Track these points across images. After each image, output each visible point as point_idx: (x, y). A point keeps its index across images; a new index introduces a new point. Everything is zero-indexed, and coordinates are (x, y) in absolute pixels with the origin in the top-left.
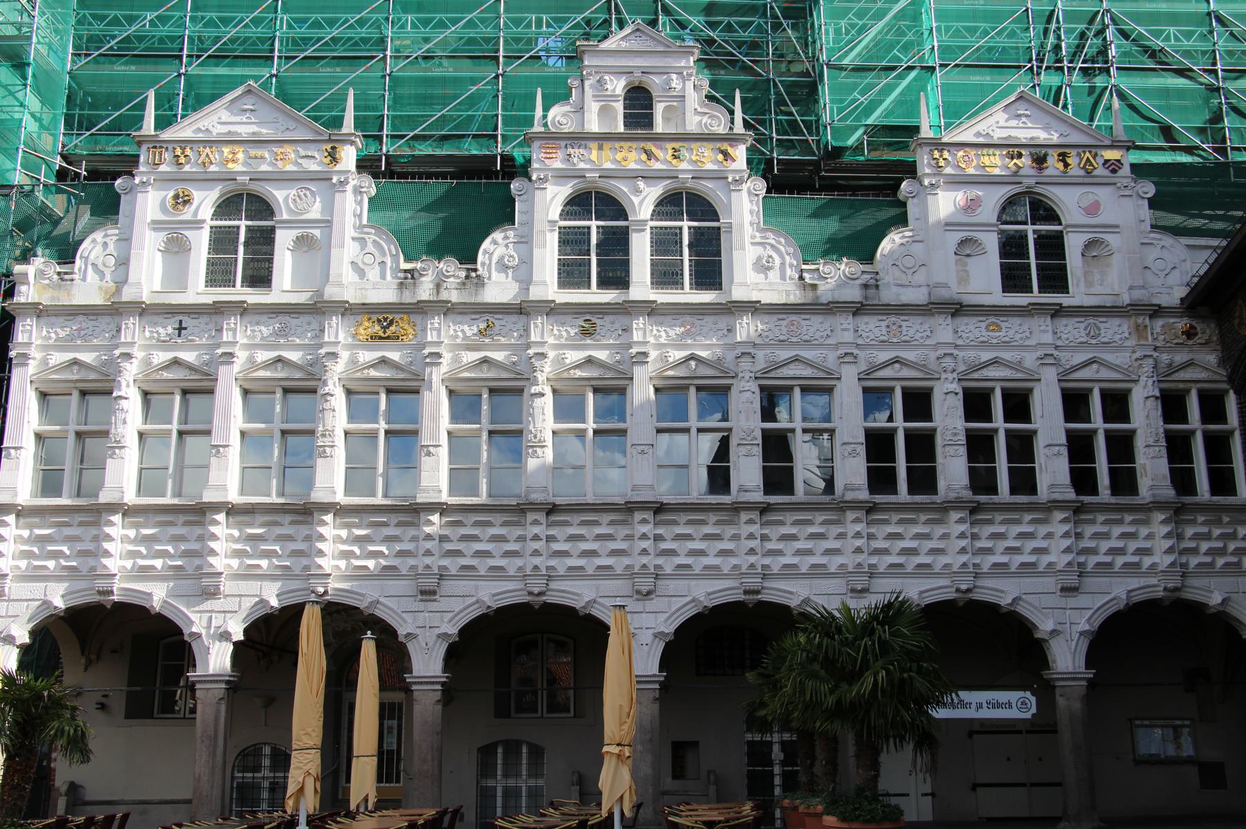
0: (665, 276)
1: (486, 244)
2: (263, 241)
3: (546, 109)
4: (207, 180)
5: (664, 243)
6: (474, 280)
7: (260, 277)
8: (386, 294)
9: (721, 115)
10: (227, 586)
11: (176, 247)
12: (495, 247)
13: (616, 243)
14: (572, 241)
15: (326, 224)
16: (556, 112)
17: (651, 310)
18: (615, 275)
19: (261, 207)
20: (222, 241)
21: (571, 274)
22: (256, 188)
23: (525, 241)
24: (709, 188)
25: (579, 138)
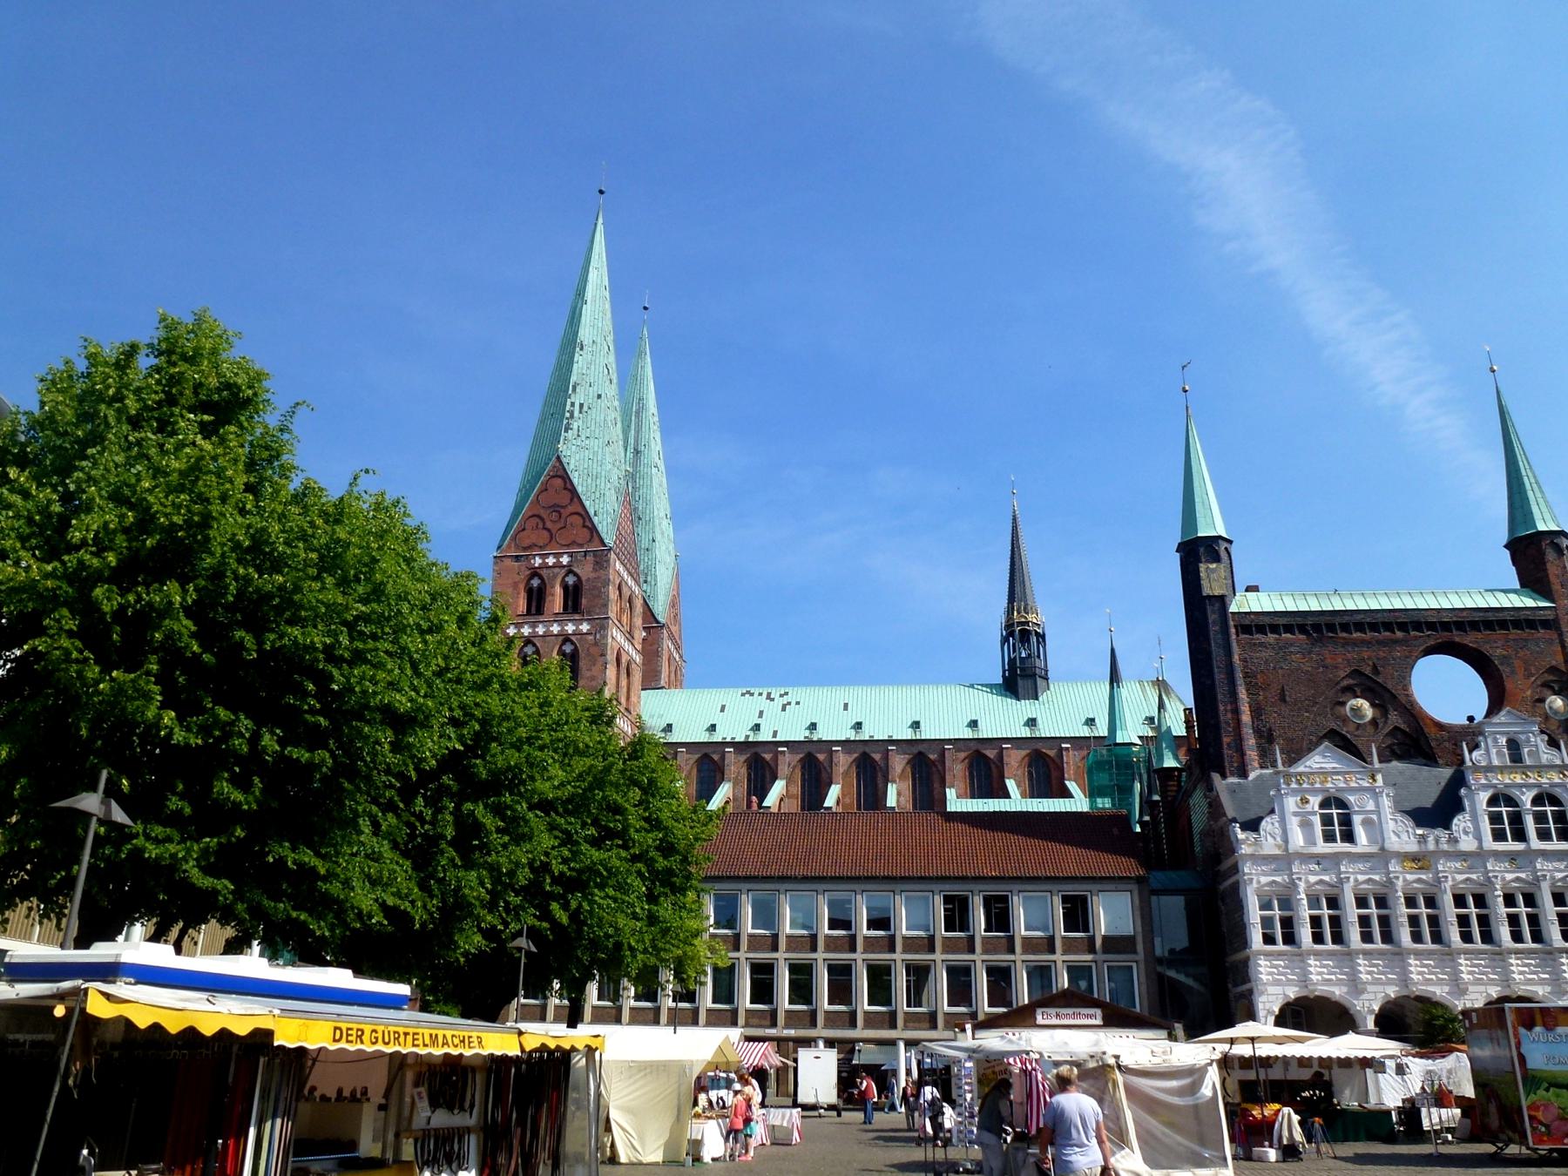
0: (1544, 835)
1: (1455, 821)
2: (1346, 821)
3: (1470, 752)
4: (1314, 792)
5: (1540, 818)
6: (1454, 840)
7: (1349, 837)
8: (1412, 847)
9: (1555, 752)
10: (1370, 988)
11: (1306, 825)
12: (1460, 822)
13: (1517, 819)
14: (1495, 819)
15: (1378, 813)
16: (1475, 754)
17: (1545, 854)
18: (1520, 835)
19: (1341, 804)
20: (1327, 821)
21: (1499, 836)
22: (1339, 795)
23: (1475, 819)
24: (1558, 791)
25: (1490, 769)
